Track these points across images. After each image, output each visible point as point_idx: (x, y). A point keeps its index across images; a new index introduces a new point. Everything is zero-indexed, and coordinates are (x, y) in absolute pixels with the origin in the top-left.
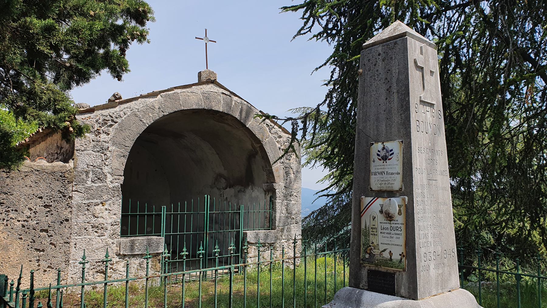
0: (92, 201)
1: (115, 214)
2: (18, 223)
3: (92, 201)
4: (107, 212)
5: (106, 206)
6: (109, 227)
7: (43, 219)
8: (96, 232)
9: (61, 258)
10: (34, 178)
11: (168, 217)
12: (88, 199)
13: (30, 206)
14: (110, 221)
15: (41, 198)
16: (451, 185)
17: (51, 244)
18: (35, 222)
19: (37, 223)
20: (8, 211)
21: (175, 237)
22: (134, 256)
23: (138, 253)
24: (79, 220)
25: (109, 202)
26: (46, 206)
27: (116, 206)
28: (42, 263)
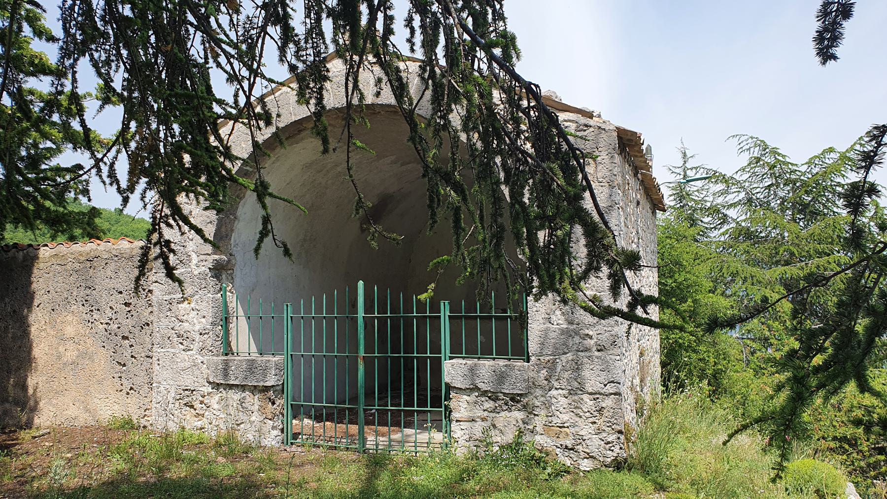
0: (174, 296)
1: (204, 317)
2: (101, 326)
3: (174, 296)
4: (195, 312)
5: (193, 305)
6: (197, 337)
7: (124, 322)
8: (181, 343)
9: (141, 379)
10: (112, 266)
11: (368, 323)
12: (170, 293)
13: (110, 304)
14: (197, 327)
15: (121, 293)
16: (102, 107)
17: (132, 356)
18: (117, 326)
19: (119, 328)
20: (92, 311)
21: (341, 360)
22: (231, 387)
23: (235, 383)
24: (162, 325)
25: (196, 297)
26: (127, 304)
27: (204, 304)
28: (124, 381)
